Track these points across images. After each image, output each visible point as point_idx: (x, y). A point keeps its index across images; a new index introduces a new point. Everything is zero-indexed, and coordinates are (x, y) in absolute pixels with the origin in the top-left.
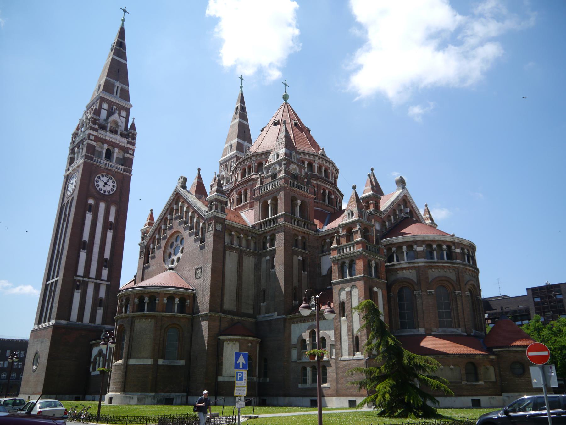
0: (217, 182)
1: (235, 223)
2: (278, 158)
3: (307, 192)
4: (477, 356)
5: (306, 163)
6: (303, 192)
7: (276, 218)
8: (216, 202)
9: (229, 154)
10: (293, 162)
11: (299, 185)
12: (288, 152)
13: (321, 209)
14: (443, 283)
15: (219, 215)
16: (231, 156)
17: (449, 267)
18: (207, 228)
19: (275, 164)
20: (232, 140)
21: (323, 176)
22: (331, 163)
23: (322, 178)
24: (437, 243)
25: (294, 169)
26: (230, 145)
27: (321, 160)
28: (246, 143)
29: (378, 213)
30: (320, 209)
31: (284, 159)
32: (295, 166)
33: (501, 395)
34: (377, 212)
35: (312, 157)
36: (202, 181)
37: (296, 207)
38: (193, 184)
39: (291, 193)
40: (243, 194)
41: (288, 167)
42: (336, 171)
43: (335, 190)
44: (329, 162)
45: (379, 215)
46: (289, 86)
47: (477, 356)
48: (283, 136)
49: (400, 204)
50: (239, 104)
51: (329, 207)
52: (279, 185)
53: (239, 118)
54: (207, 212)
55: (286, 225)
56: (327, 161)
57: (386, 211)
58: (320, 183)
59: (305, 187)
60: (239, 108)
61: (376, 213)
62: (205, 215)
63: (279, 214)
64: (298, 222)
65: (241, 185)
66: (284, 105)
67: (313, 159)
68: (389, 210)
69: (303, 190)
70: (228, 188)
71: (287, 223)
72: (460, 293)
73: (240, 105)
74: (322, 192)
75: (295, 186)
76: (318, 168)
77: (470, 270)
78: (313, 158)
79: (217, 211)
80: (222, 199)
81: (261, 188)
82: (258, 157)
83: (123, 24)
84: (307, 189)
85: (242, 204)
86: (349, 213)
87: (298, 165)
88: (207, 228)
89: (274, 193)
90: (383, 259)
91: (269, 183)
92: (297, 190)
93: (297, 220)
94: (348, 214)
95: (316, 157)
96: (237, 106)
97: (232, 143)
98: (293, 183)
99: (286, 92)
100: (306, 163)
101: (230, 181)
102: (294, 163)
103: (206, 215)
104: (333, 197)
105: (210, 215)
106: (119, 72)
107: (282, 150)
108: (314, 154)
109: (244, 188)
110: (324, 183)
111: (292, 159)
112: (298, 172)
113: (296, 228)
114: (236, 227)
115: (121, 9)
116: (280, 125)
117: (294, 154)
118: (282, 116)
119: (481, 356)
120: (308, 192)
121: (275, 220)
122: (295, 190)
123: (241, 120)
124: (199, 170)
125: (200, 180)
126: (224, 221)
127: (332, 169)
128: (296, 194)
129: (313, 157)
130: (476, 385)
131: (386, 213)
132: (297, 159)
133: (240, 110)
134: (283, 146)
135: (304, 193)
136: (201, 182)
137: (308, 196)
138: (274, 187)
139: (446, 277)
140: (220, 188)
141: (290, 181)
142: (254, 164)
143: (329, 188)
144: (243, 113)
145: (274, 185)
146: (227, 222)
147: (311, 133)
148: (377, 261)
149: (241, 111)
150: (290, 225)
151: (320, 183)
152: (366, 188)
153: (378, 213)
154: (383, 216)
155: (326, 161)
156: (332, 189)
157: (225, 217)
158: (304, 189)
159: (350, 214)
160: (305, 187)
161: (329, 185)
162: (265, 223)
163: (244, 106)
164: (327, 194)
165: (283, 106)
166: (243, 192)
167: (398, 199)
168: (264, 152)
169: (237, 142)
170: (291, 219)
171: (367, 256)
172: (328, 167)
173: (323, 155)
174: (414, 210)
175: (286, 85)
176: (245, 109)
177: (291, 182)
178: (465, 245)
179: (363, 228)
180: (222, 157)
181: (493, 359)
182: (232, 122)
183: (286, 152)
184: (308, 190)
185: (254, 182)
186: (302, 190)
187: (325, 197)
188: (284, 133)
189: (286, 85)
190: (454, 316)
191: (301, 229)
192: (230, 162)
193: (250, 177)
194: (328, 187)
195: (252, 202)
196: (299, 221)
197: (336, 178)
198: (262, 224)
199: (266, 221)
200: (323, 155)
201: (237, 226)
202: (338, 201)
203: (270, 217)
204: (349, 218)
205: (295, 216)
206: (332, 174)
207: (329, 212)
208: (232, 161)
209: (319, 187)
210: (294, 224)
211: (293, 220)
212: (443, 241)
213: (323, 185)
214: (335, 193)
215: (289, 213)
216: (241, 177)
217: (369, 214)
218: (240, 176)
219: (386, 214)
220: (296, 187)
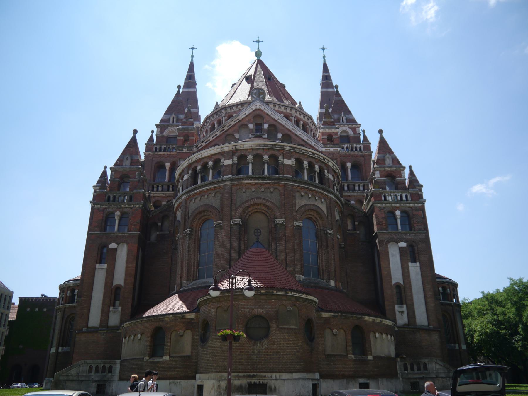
4: (166, 318)
17: (210, 189)
24: (201, 163)
33: (194, 378)
34: (182, 148)
45: (187, 150)
47: (166, 317)
49: (247, 123)
64: (162, 186)
72: (220, 223)
77: (251, 184)
83: (192, 60)
90: (137, 206)
92: (164, 154)
99: (258, 49)
106: (188, 100)
113: (156, 194)
115: (189, 48)
119: (171, 316)
130: (158, 362)
139: (205, 205)
148: (125, 210)
153: (184, 149)
167: (238, 119)
170: (151, 186)
171: (104, 209)
174: (279, 123)
179: (119, 176)
181: (192, 319)
190: (194, 259)
191: (163, 194)
196: (164, 186)
210: (157, 190)
211: (155, 186)
212: (208, 157)
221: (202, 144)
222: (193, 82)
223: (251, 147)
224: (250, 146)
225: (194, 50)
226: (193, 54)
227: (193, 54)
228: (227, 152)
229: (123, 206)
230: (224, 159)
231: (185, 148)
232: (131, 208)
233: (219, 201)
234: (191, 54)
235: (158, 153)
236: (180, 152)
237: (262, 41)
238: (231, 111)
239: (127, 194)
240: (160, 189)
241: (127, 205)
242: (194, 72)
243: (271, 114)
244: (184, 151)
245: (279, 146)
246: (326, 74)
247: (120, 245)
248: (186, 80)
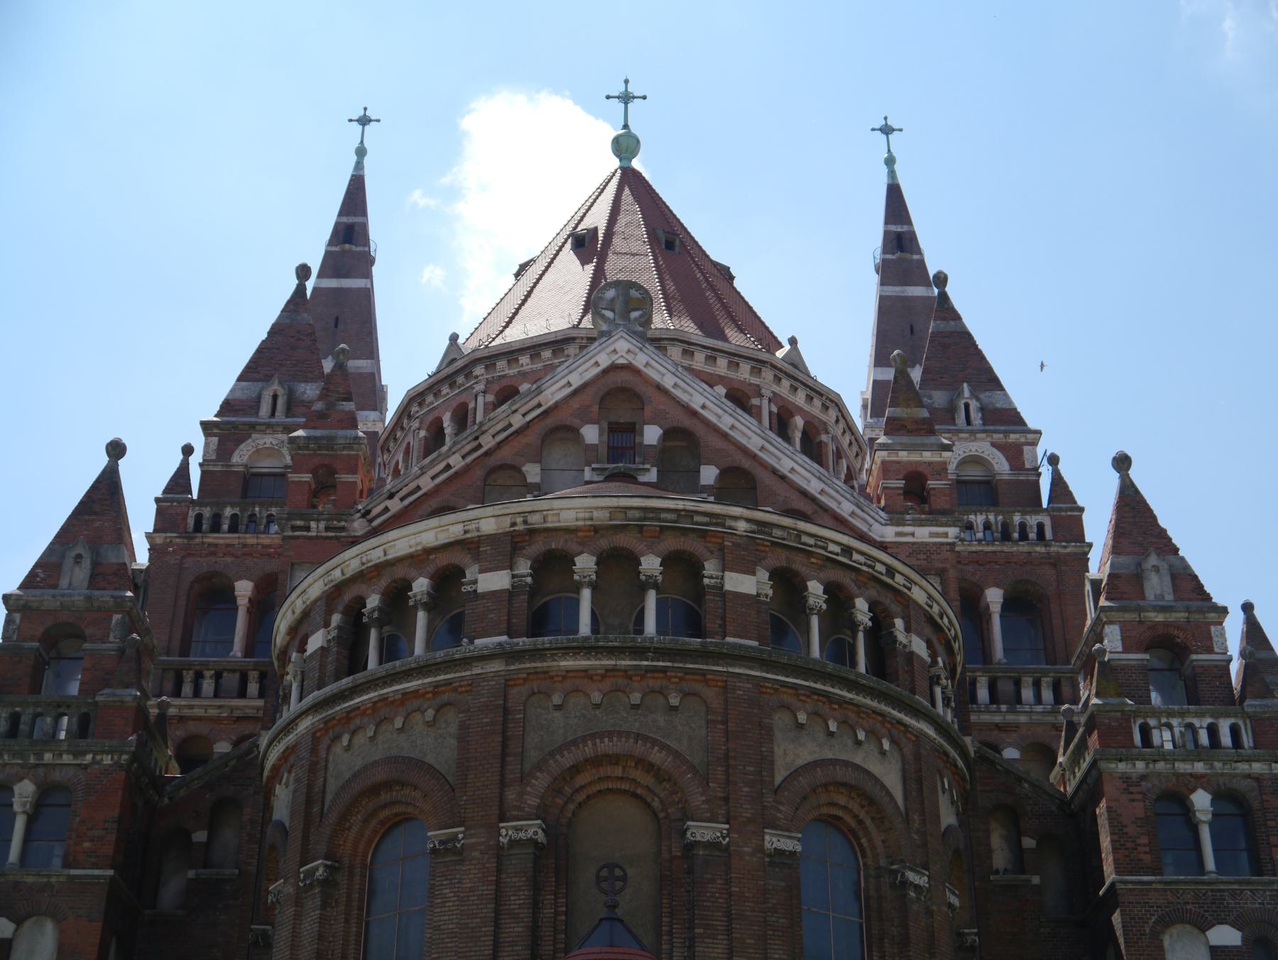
14: (384, 807)
17: (416, 694)
24: (383, 583)
49: (575, 422)
64: (218, 676)
72: (454, 838)
77: (586, 673)
83: (359, 165)
90: (107, 760)
92: (228, 541)
99: (626, 126)
113: (192, 707)
148: (57, 776)
153: (313, 524)
167: (539, 405)
170: (171, 676)
178: (567, 530)
191: (220, 707)
196: (225, 674)
210: (197, 693)
211: (188, 677)
221: (388, 503)
222: (359, 253)
223: (591, 519)
224: (587, 515)
225: (366, 127)
226: (362, 142)
227: (362, 142)
228: (492, 539)
229: (48, 757)
230: (476, 568)
231: (318, 521)
232: (86, 767)
233: (453, 742)
234: (356, 144)
235: (205, 540)
236: (297, 537)
239: (68, 706)
240: (208, 686)
241: (68, 752)
242: (364, 213)
243: (676, 385)
244: (313, 534)
245: (706, 519)
246: (899, 230)
247: (28, 924)
248: (331, 242)
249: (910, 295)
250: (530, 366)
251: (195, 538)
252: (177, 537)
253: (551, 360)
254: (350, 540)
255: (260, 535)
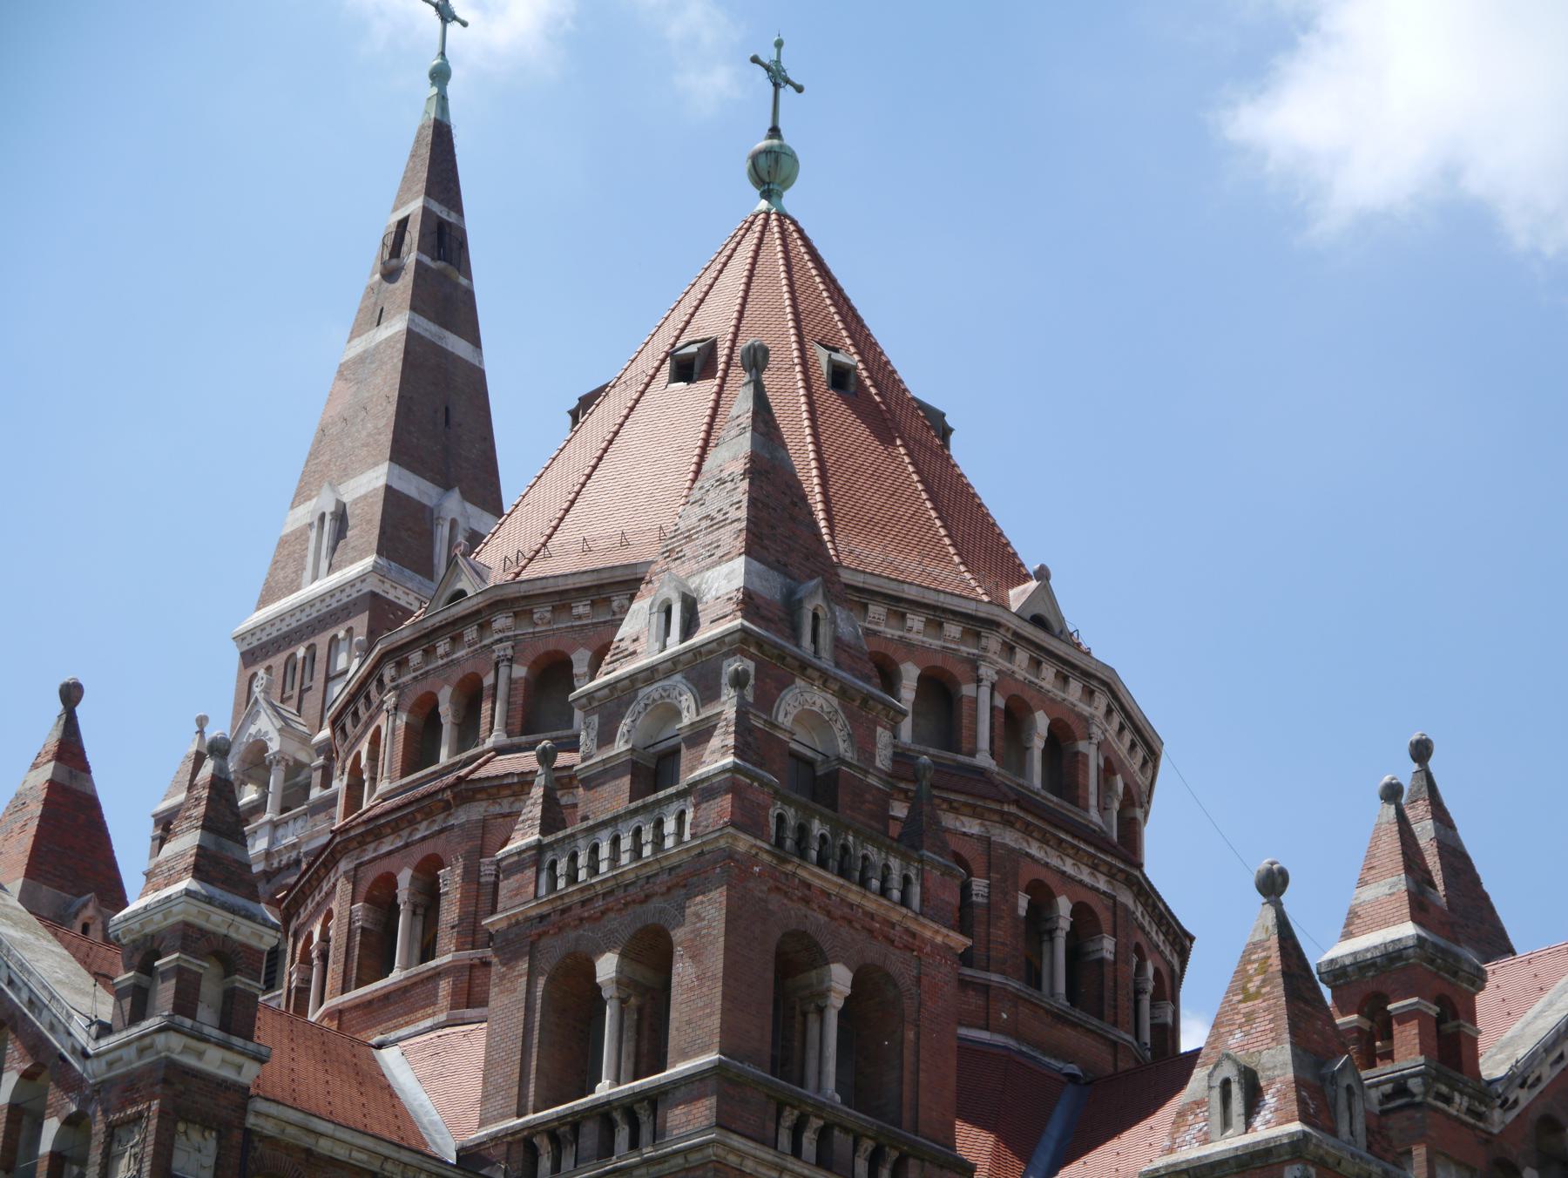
0: (205, 794)
1: (326, 1127)
2: (689, 628)
3: (904, 901)
5: (910, 674)
6: (872, 903)
7: (655, 1100)
8: (184, 950)
9: (315, 578)
10: (803, 667)
11: (845, 848)
12: (772, 587)
13: (1012, 1043)
15: (200, 1055)
16: (331, 593)
18: (95, 1156)
19: (668, 674)
20: (346, 474)
21: (1037, 781)
22: (1101, 683)
23: (1024, 801)
25: (810, 718)
26: (330, 508)
27: (1022, 656)
28: (453, 505)
29: (1457, 1097)
30: (999, 1039)
31: (740, 642)
32: (821, 700)
34: (1452, 1088)
35: (953, 630)
36: (90, 780)
37: (813, 1019)
38: (19, 803)
39: (775, 901)
40: (403, 894)
41: (766, 701)
42: (1140, 752)
43: (1126, 898)
44: (1086, 675)
45: (1470, 1111)
46: (799, 89)
48: (739, 467)
50: (415, 206)
51: (1075, 1025)
52: (687, 836)
53: (413, 308)
54: (105, 1030)
55: (732, 1159)
56: (1074, 667)
57: (1520, 1077)
58: (1009, 838)
59: (895, 864)
60: (413, 234)
61: (1440, 1096)
62: (85, 1055)
63: (679, 1068)
64: (824, 1135)
65: (396, 827)
66: (757, 227)
67: (967, 650)
68: (1548, 1074)
69: (875, 884)
70: (294, 846)
71: (736, 1141)
73: (426, 211)
74: (1022, 912)
75: (814, 854)
76: (1001, 719)
78: (962, 641)
79: (188, 1022)
80: (233, 935)
81: (549, 857)
82: (542, 612)
84: (906, 880)
85: (396, 975)
86: (1226, 1083)
87: (844, 693)
88: (95, 1156)
89: (648, 897)
91: (615, 820)
92: (826, 886)
93: (816, 1123)
94: (1216, 1095)
95: (984, 633)
96: (400, 215)
97: (346, 499)
98: (803, 831)
99: (775, 132)
100: (910, 674)
101: (316, 793)
102: (809, 671)
103: (98, 1055)
104: (1108, 946)
105: (130, 1053)
107: (724, 568)
108: (969, 607)
109: (419, 853)
110: (1044, 840)
111: (795, 636)
112: (843, 747)
114: (333, 1161)
116: (723, 379)
117: (814, 602)
118: (741, 313)
120: (916, 901)
121: (644, 1116)
122: (809, 886)
123: (428, 328)
124: (71, 694)
125: (72, 776)
126: (243, 1109)
127: (1105, 729)
128: (823, 918)
129: (965, 632)
131: (1525, 1097)
132: (838, 642)
133: (419, 249)
134: (732, 537)
135: (882, 911)
136: (75, 786)
137: (914, 935)
138: (647, 851)
140: (229, 843)
141: (773, 812)
142: (503, 671)
143: (1081, 882)
144: (441, 274)
145: (647, 836)
146: (264, 1118)
147: (959, 449)
149: (426, 260)
150: (761, 1162)
151: (1009, 838)
152: (1369, 893)
153: (1457, 1097)
154: (1498, 1120)
155: (1066, 671)
156: (1102, 884)
157: (249, 1073)
158: (884, 880)
159: (1236, 1090)
160: (895, 864)
161: (1077, 855)
162: (561, 1135)
163: (452, 218)
164: (1065, 924)
165: (751, 240)
166: (404, 878)
168: (586, 581)
169: (388, 488)
170: (772, 1108)
172: (1080, 716)
173: (1039, 621)
175: (778, 78)
176: (462, 245)
177: (781, 819)
180: (263, 602)
182: (356, 333)
183: (758, 586)
184: (916, 890)
185: (496, 809)
186: (864, 883)
187: (1046, 947)
188: (744, 444)
189: (778, 78)
192: (322, 641)
193: (466, 763)
194: (1069, 867)
195: (472, 967)
196: (836, 1132)
197: (1135, 803)
198: (543, 1144)
199: (575, 1122)
200: (1043, 619)
201: (341, 1153)
202: (1150, 986)
203: (604, 1089)
204: (1226, 1124)
205: (802, 1084)
206: (1109, 769)
207: (1073, 1068)
208: (341, 634)
209: (1001, 863)
210: (796, 1151)
211: (790, 1117)
213: (1035, 850)
214: (1121, 920)
215: (759, 1065)
216: (398, 765)
217: (1387, 1098)
218: (392, 752)
219: (1523, 1104)
220: (822, 863)
231: (1462, 1093)
235: (799, 871)
237: (798, 82)
238: (891, 632)
246: (444, 216)
249: (450, 348)
250: (920, 637)
251: (789, 862)
252: (767, 852)
253: (955, 642)
254: (1485, 1136)
255: (868, 894)
